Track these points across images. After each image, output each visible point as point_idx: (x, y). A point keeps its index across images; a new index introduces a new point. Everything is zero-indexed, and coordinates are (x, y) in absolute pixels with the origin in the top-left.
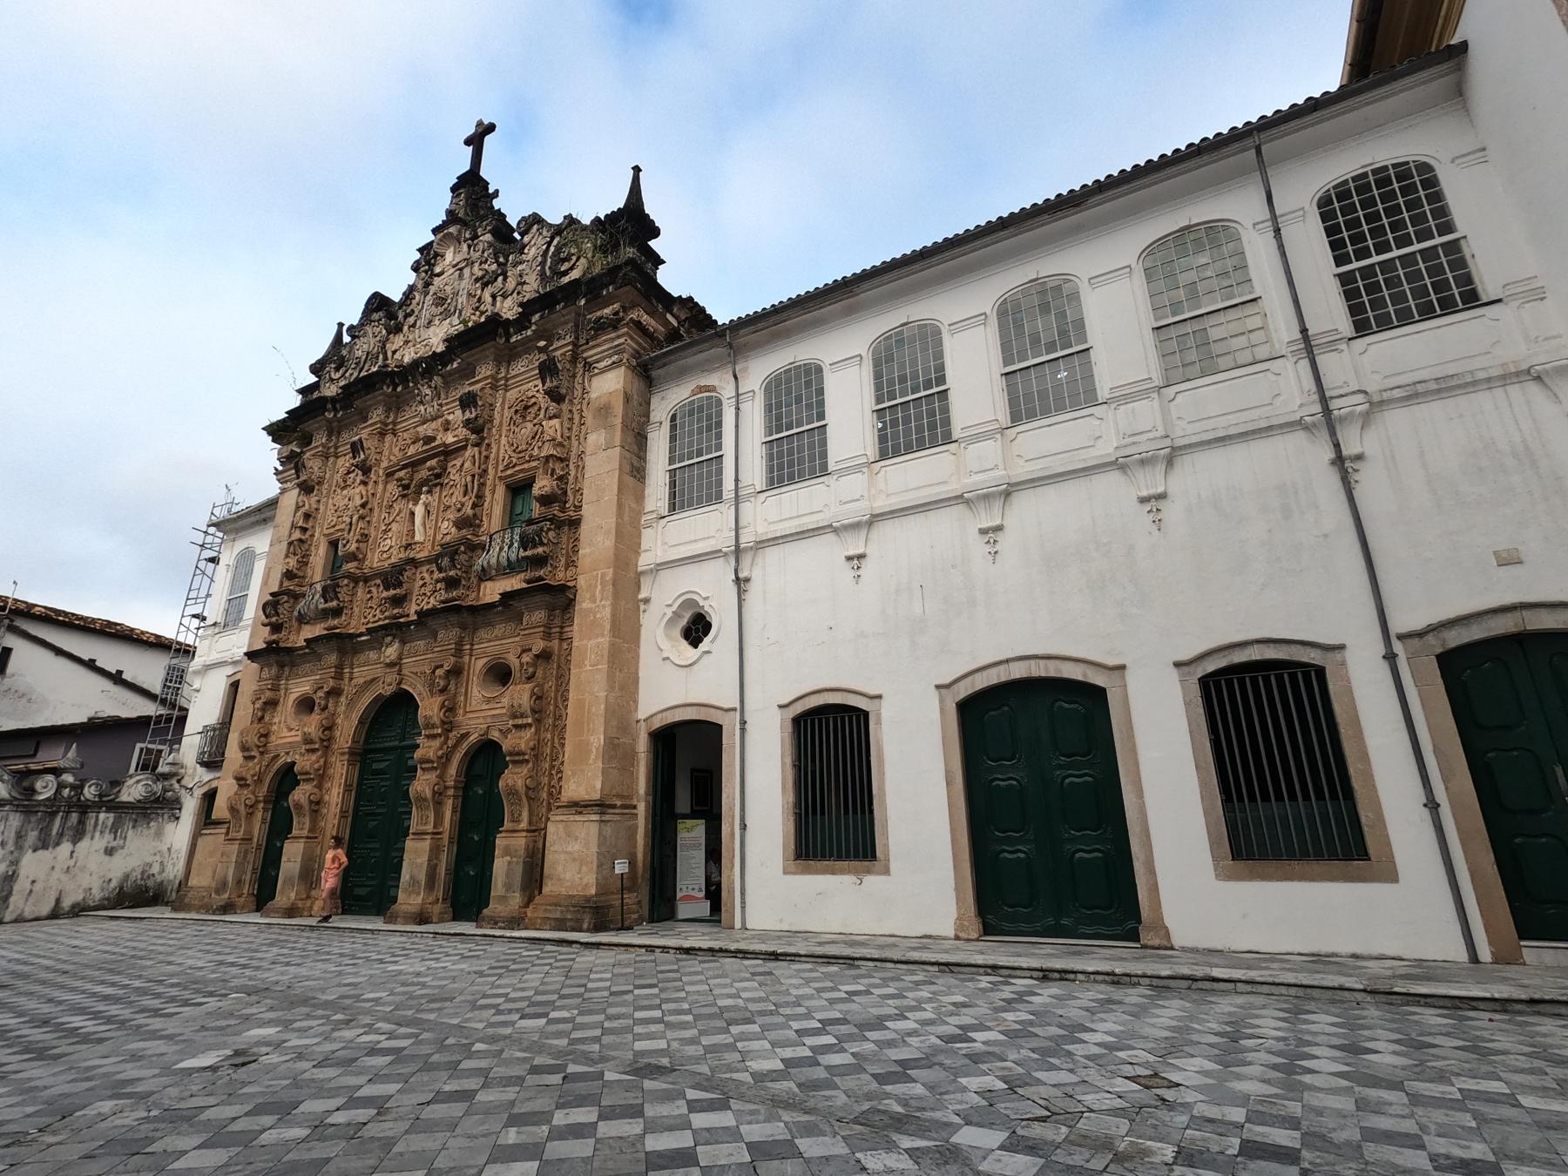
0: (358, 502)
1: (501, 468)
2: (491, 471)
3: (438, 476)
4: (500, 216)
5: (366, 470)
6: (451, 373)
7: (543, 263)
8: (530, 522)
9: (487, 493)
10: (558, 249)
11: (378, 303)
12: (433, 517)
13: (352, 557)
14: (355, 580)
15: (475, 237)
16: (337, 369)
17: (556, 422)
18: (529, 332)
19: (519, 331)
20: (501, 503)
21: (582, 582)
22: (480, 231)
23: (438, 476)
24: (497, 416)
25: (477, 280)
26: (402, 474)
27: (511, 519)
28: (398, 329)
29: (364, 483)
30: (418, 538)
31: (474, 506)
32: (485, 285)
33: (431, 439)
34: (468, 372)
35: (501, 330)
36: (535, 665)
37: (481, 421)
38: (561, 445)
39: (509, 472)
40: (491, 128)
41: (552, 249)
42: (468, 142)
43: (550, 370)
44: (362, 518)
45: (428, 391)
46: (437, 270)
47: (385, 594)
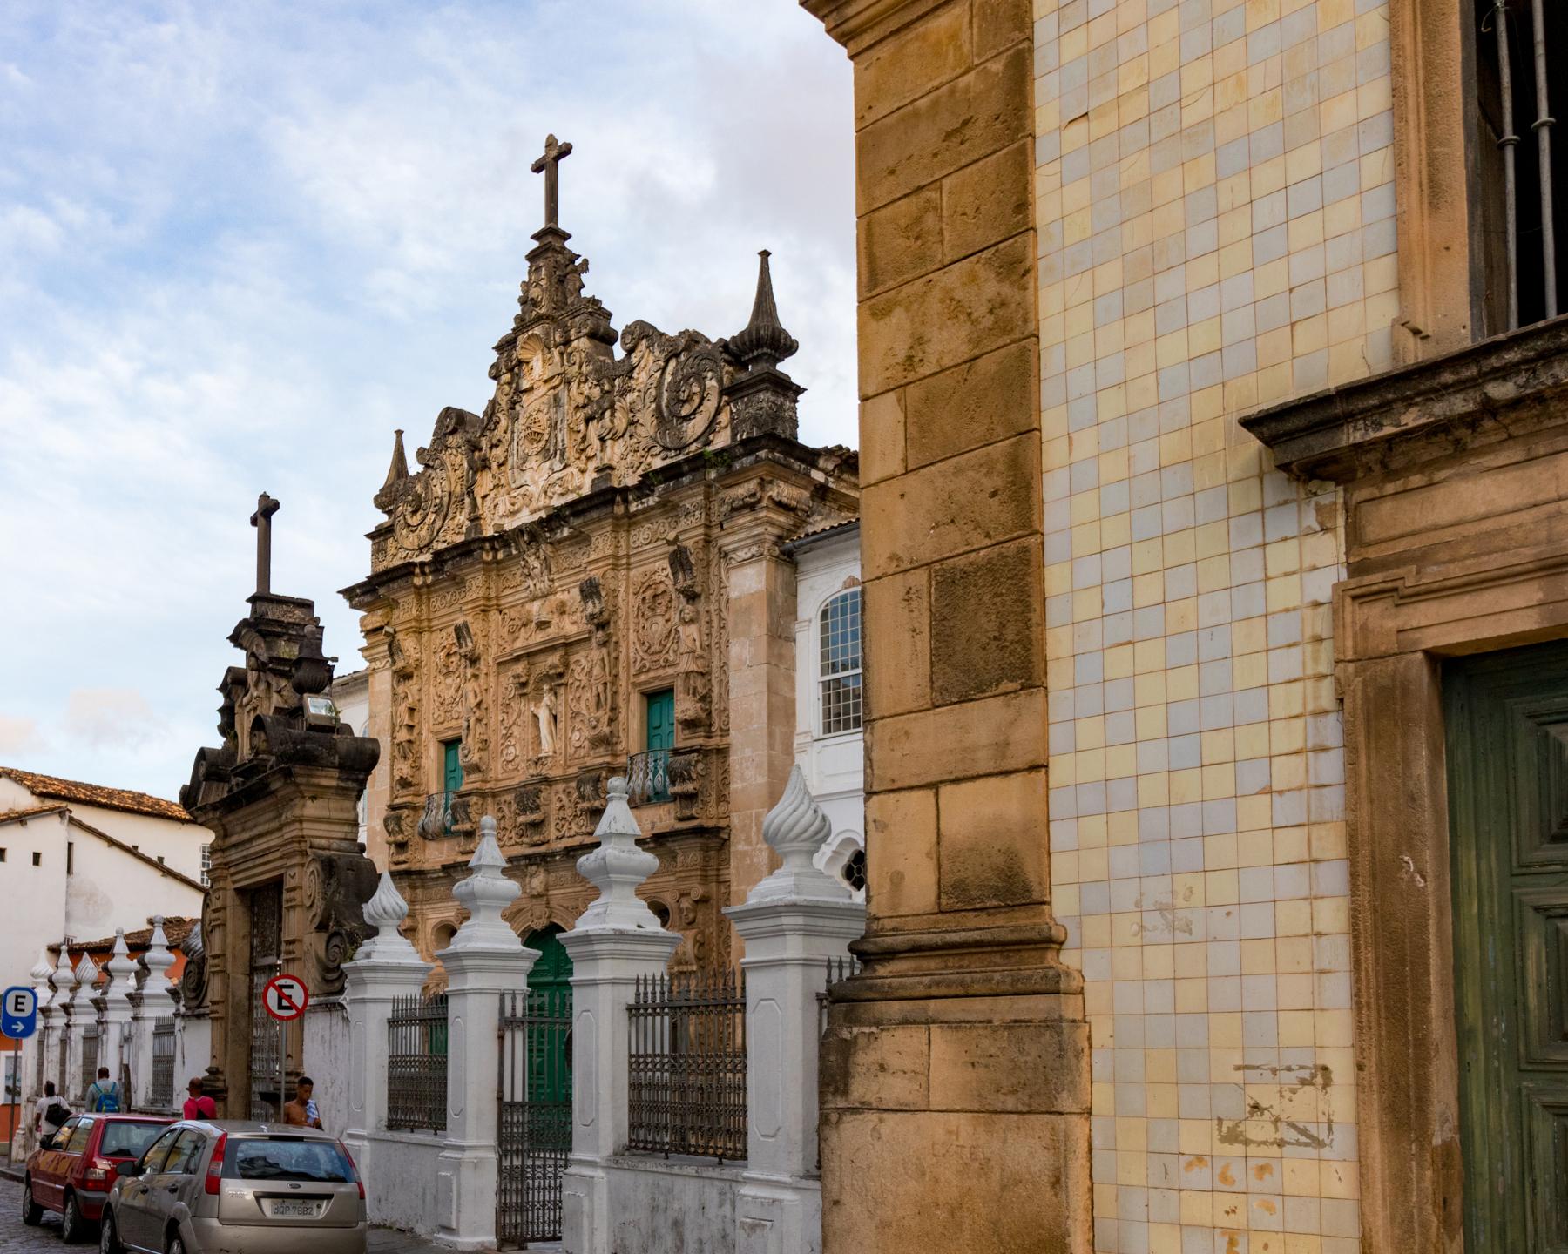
0: (473, 702)
1: (633, 671)
2: (623, 676)
3: (561, 675)
4: (597, 310)
5: (473, 660)
6: (559, 542)
7: (657, 399)
8: (677, 752)
9: (621, 703)
10: (675, 387)
11: (453, 422)
12: (561, 725)
13: (476, 768)
14: (482, 795)
15: (567, 343)
16: (414, 513)
17: (693, 629)
18: (652, 501)
19: (638, 498)
20: (638, 715)
21: (735, 820)
23: (561, 675)
24: (622, 604)
25: (577, 408)
26: (519, 668)
27: (652, 731)
28: (485, 465)
29: (476, 676)
30: (547, 746)
31: (611, 721)
32: (588, 420)
33: (543, 625)
34: (581, 539)
35: (618, 498)
36: (695, 911)
37: (606, 615)
38: (701, 657)
39: (643, 678)
40: (566, 150)
41: (668, 378)
42: (537, 168)
43: (681, 565)
44: (479, 720)
45: (536, 563)
47: (522, 819)
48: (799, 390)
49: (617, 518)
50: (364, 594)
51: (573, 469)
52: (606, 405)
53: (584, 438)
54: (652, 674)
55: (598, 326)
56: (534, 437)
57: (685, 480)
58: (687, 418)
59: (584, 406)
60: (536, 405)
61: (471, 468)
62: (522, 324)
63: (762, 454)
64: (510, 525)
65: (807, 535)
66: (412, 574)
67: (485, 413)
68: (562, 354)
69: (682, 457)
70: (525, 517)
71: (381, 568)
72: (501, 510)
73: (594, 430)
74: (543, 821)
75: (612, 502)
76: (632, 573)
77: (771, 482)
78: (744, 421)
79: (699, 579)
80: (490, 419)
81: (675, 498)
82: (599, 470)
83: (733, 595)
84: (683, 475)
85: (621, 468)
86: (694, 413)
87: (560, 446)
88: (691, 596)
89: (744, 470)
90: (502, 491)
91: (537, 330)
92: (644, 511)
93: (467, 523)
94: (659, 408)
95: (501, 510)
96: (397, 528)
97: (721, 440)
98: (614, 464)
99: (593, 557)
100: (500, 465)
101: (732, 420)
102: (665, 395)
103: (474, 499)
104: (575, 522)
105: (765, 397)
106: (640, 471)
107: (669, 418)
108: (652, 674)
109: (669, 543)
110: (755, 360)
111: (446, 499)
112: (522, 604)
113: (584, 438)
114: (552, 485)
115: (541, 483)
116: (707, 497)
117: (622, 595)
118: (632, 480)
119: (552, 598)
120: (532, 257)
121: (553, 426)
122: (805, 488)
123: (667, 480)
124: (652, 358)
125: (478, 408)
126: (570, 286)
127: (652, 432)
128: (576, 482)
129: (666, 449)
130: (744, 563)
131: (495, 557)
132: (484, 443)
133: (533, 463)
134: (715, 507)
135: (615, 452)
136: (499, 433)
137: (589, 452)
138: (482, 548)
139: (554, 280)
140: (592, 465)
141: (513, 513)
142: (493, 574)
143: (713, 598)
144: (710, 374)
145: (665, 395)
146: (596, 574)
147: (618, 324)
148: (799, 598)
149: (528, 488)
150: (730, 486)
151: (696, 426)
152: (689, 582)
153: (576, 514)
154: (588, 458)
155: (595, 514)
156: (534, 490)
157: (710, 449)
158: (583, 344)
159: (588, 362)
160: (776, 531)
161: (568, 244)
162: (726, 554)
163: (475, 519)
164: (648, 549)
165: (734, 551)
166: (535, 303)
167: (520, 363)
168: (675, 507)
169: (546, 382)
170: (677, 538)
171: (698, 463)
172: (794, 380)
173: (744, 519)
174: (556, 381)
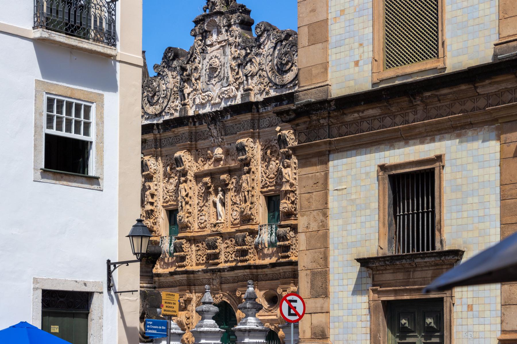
35: (254, 107)
39: (265, 190)
54: (270, 188)
58: (287, 72)
60: (214, 53)
64: (201, 112)
72: (197, 101)
74: (219, 253)
82: (245, 90)
94: (273, 64)
102: (276, 60)
108: (270, 188)
113: (238, 73)
115: (217, 91)
132: (188, 67)
136: (196, 64)
145: (276, 60)
169: (219, 43)
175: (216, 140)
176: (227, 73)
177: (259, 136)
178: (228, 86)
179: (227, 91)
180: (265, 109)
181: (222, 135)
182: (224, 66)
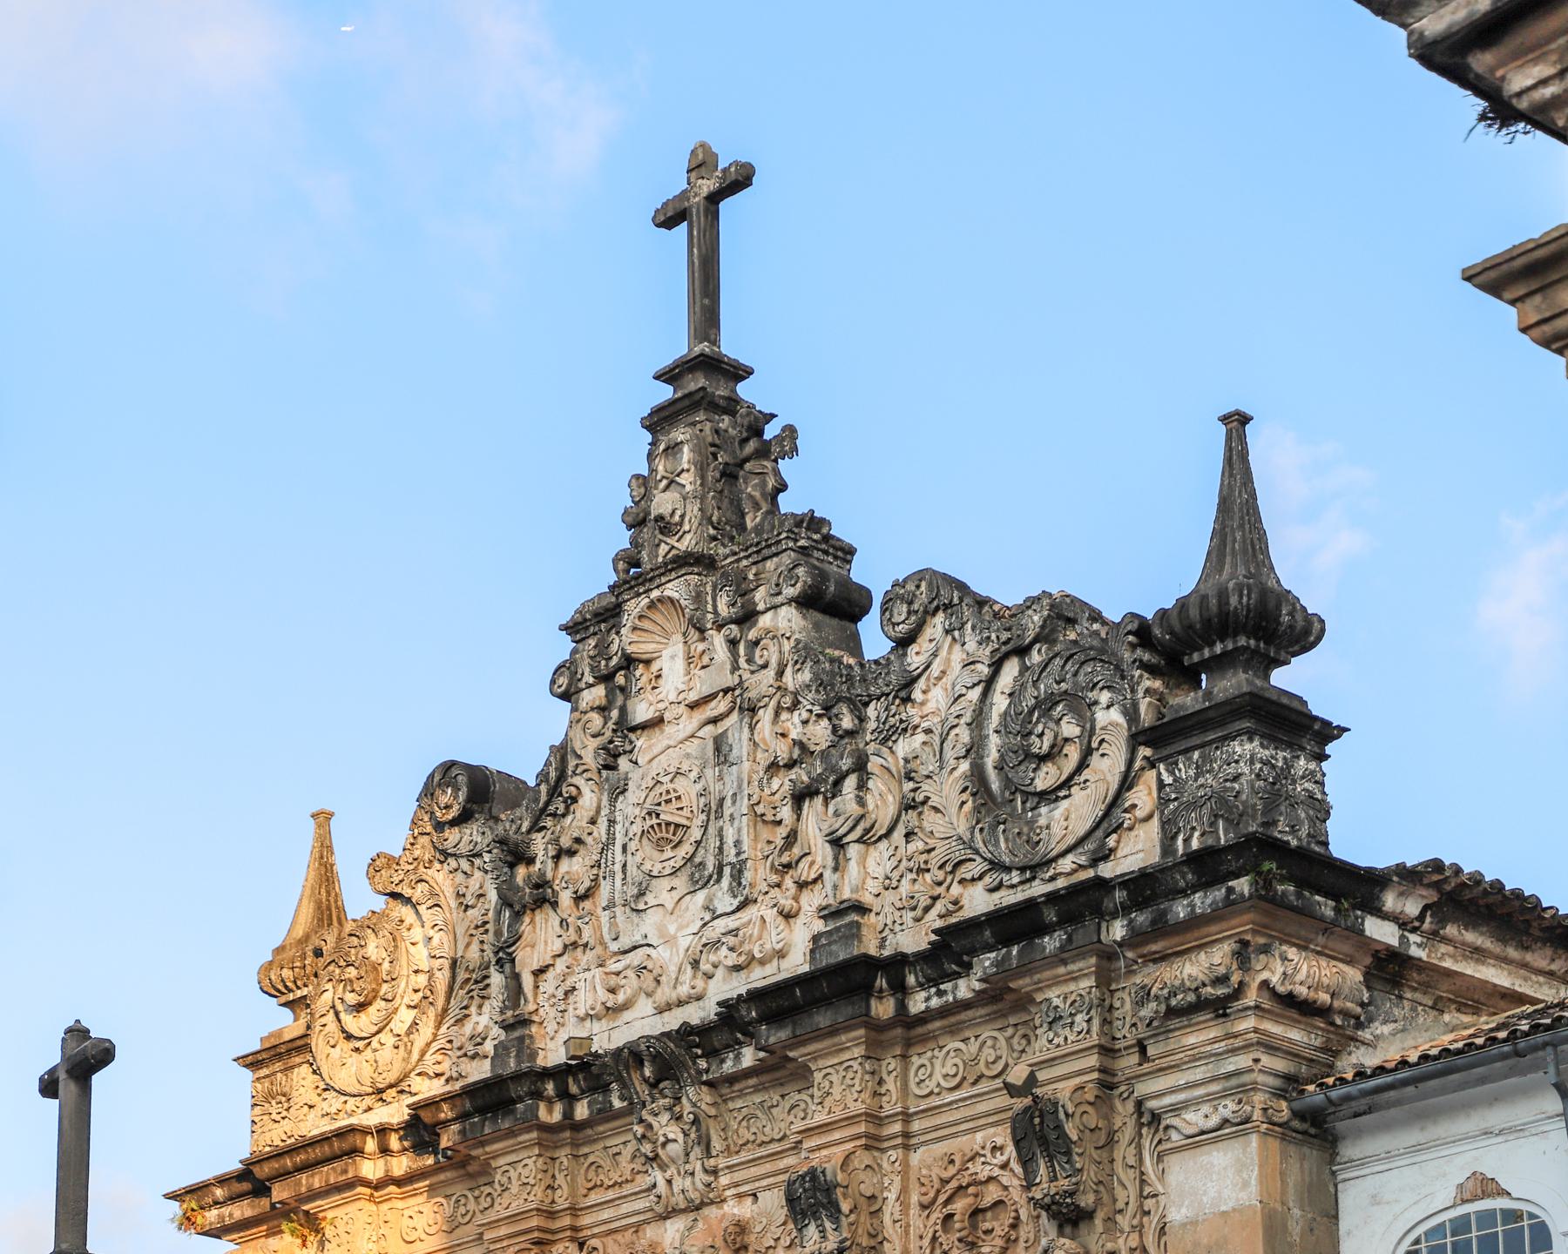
4: (819, 542)
6: (731, 1079)
7: (974, 750)
10: (1020, 724)
15: (747, 617)
18: (964, 989)
19: (932, 981)
22: (760, 597)
24: (890, 1230)
25: (773, 767)
28: (542, 896)
32: (799, 798)
35: (881, 982)
41: (1000, 703)
42: (669, 218)
43: (1044, 1142)
45: (673, 1131)
46: (641, 711)
48: (1327, 732)
49: (877, 1028)
50: (233, 1199)
51: (763, 910)
52: (846, 764)
53: (791, 838)
55: (821, 576)
56: (665, 833)
57: (1050, 943)
59: (791, 765)
60: (670, 760)
61: (505, 902)
62: (634, 574)
63: (1243, 885)
64: (607, 1038)
65: (1360, 1075)
66: (356, 1152)
67: (543, 776)
68: (733, 643)
69: (1038, 889)
70: (642, 1023)
71: (276, 1135)
72: (583, 1001)
73: (815, 822)
75: (866, 991)
76: (915, 1158)
77: (1265, 950)
78: (1194, 805)
79: (1090, 1175)
80: (554, 791)
81: (1022, 984)
83: (1176, 1215)
84: (1047, 930)
85: (885, 909)
86: (1067, 784)
87: (730, 855)
88: (1069, 1216)
89: (1195, 921)
90: (587, 958)
91: (675, 589)
92: (944, 1012)
93: (496, 1031)
94: (978, 774)
95: (583, 1001)
96: (318, 1043)
97: (1137, 850)
98: (867, 899)
99: (820, 1117)
100: (579, 898)
101: (1163, 802)
102: (994, 742)
103: (516, 977)
104: (777, 1036)
105: (1246, 753)
106: (933, 920)
107: (1001, 798)
109: (1012, 1090)
110: (1217, 665)
111: (442, 979)
112: (637, 1228)
113: (791, 838)
114: (715, 945)
115: (684, 942)
116: (1105, 980)
117: (891, 1210)
118: (913, 939)
119: (712, 1212)
120: (659, 421)
121: (714, 810)
122: (1349, 962)
123: (1007, 942)
124: (958, 656)
125: (526, 765)
126: (751, 489)
127: (962, 828)
128: (772, 941)
129: (996, 865)
130: (1201, 1139)
131: (568, 1114)
132: (540, 845)
133: (661, 893)
134: (1124, 1003)
135: (867, 872)
136: (575, 823)
137: (805, 871)
138: (538, 1095)
139: (711, 475)
140: (812, 900)
141: (613, 1011)
142: (563, 1154)
143: (1124, 1222)
144: (1105, 697)
145: (994, 742)
146: (828, 1157)
147: (874, 572)
148: (1344, 1225)
149: (653, 952)
150: (1162, 958)
151: (1070, 817)
152: (1064, 1184)
153: (774, 1018)
154: (802, 885)
155: (823, 1019)
156: (668, 958)
157: (1107, 870)
158: (787, 621)
159: (799, 664)
160: (1281, 1065)
161: (744, 390)
162: (1156, 1118)
163: (517, 1024)
164: (954, 1097)
165: (1176, 1109)
166: (666, 527)
167: (629, 662)
168: (1024, 1002)
169: (693, 706)
170: (1031, 1080)
171: (1083, 903)
172: (1316, 709)
173: (1200, 1035)
174: (721, 705)
175: (678, 1184)
176: (737, 843)
177: (906, 1135)
178: (738, 909)
179: (734, 932)
180: (940, 993)
181: (709, 1156)
182: (719, 816)
